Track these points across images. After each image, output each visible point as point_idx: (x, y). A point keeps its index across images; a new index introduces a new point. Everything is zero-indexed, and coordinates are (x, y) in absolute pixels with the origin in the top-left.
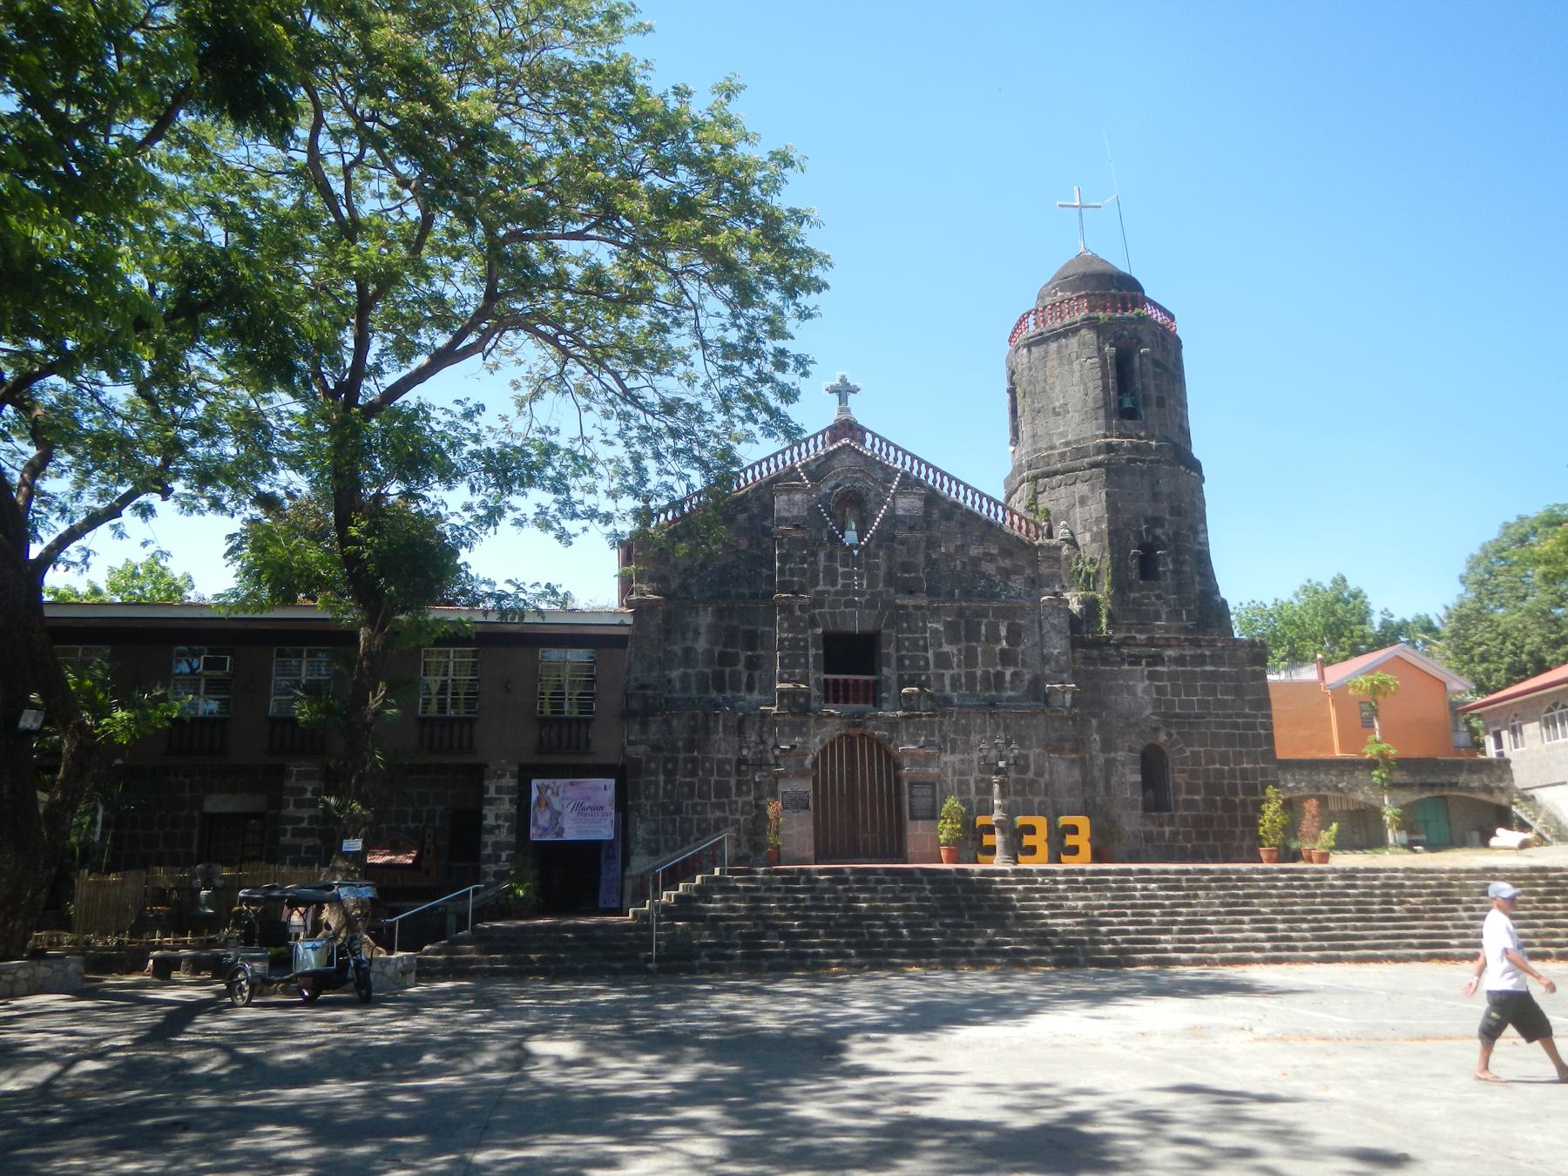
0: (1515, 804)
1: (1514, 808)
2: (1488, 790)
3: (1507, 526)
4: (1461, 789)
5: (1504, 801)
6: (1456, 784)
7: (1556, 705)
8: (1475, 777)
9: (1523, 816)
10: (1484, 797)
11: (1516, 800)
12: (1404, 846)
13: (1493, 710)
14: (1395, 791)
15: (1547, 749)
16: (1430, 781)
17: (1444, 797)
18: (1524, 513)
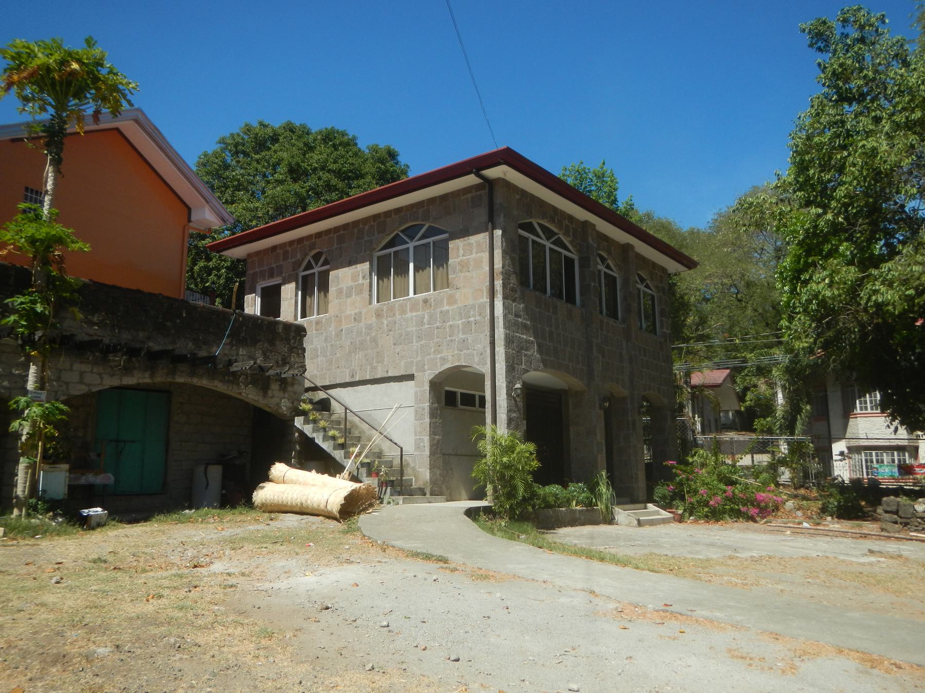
0: (304, 413)
1: (298, 422)
2: (260, 379)
3: (248, 129)
4: (213, 373)
5: (285, 406)
6: (212, 359)
7: (411, 233)
8: (242, 351)
9: (319, 441)
10: (250, 394)
11: (306, 407)
12: (53, 506)
13: (274, 248)
14: (63, 361)
15: (379, 315)
16: (155, 346)
17: (165, 393)
18: (266, 123)
